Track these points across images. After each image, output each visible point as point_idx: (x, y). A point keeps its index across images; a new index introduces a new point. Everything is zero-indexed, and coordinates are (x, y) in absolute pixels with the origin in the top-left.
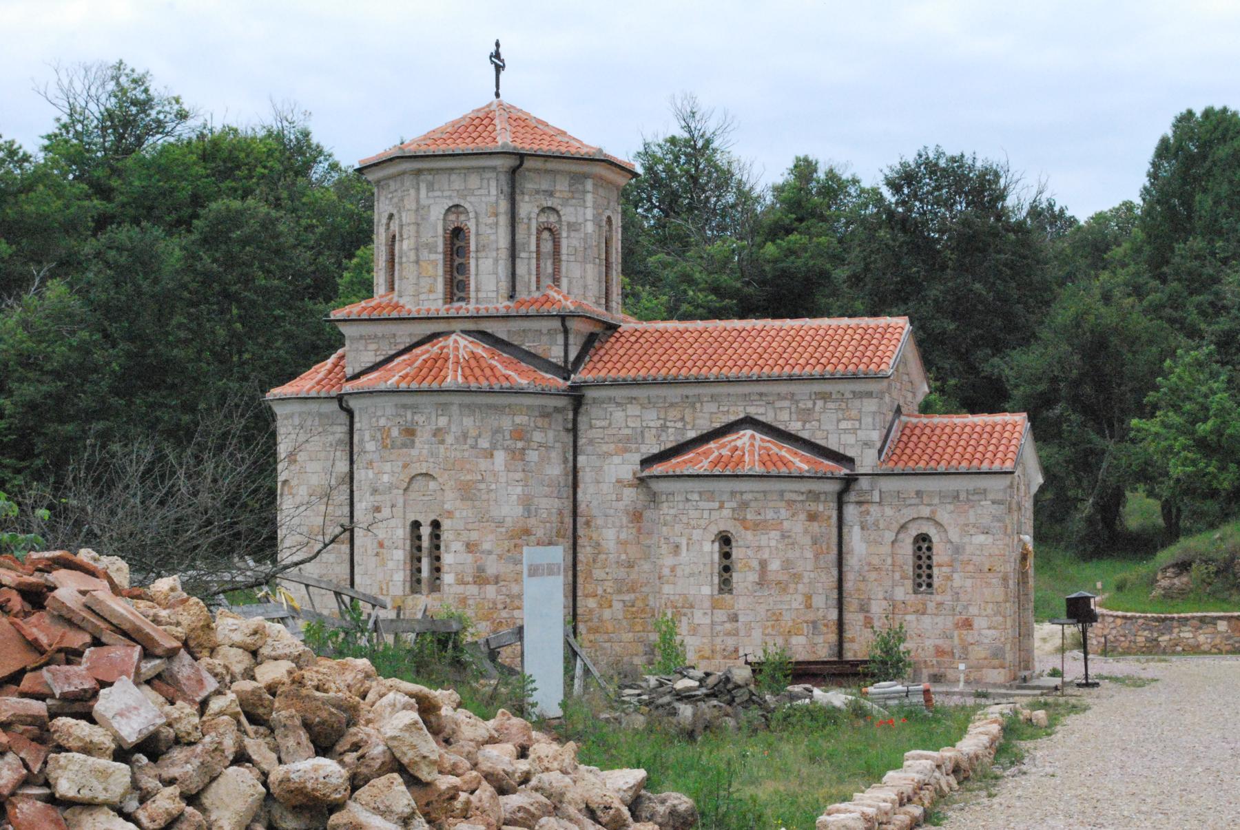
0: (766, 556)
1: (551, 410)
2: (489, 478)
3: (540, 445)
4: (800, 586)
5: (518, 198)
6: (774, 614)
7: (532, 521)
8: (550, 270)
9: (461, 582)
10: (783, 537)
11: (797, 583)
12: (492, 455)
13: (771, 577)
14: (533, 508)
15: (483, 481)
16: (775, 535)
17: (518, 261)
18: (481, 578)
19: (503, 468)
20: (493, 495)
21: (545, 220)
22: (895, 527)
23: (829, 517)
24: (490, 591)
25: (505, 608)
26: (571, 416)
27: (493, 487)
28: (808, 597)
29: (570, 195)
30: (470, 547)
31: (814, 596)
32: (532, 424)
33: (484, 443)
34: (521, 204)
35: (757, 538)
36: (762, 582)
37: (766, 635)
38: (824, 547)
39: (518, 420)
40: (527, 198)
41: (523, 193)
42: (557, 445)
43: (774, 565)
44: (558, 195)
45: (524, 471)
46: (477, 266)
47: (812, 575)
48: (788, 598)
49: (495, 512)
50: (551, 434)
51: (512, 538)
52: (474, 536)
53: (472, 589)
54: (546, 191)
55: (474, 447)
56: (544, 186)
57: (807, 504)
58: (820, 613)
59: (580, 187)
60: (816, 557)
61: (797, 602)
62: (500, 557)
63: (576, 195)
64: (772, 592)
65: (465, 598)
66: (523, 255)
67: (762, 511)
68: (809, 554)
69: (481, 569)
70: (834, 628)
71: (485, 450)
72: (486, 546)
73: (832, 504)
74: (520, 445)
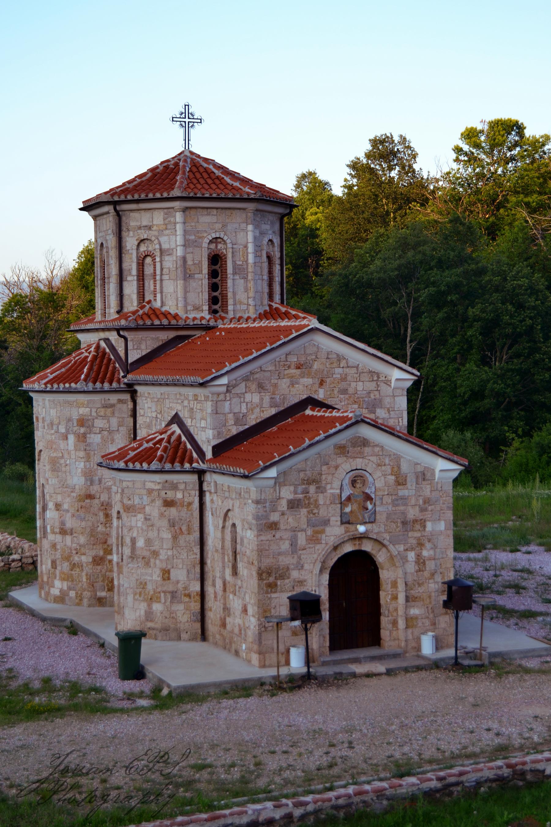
0: (135, 535)
1: (115, 402)
2: (66, 456)
3: (102, 430)
4: (158, 562)
5: (124, 234)
6: (141, 583)
7: (94, 490)
8: (152, 288)
9: (53, 532)
10: (146, 519)
11: (156, 559)
12: (67, 438)
13: (138, 552)
14: (96, 478)
15: (62, 457)
16: (140, 516)
17: (125, 284)
18: (63, 532)
19: (73, 448)
20: (68, 468)
21: (145, 249)
22: (222, 515)
23: (190, 504)
24: (68, 538)
25: (77, 553)
26: (130, 405)
27: (68, 462)
28: (166, 574)
29: (164, 227)
30: (58, 506)
31: (172, 571)
32: (94, 414)
33: (62, 430)
34: (128, 239)
35: (129, 519)
36: (133, 557)
37: (137, 600)
38: (184, 528)
39: (82, 411)
40: (131, 233)
41: (128, 230)
42: (121, 429)
43: (140, 543)
44: (155, 228)
45: (85, 450)
46: (109, 289)
47: (170, 553)
48: (149, 571)
49: (69, 482)
50: (114, 422)
51: (80, 500)
52: (59, 498)
53: (59, 538)
54: (146, 226)
55: (57, 432)
56: (145, 223)
57: (163, 493)
58: (180, 586)
59: (172, 219)
60: (175, 538)
61: (156, 576)
62: (73, 515)
63: (169, 227)
64: (140, 564)
65: (55, 544)
66: (129, 278)
67: (131, 497)
68: (167, 535)
69: (63, 523)
70: (198, 598)
71: (63, 433)
72: (66, 506)
73: (193, 493)
74: (82, 430)
